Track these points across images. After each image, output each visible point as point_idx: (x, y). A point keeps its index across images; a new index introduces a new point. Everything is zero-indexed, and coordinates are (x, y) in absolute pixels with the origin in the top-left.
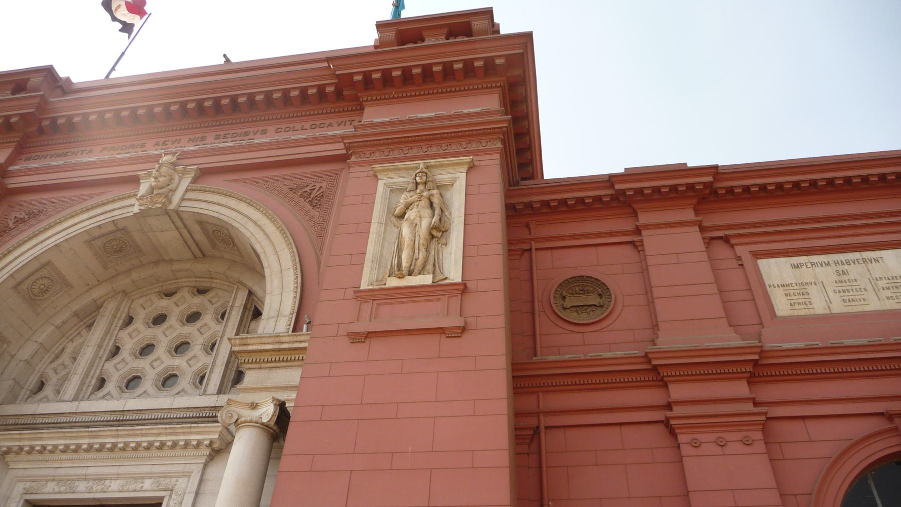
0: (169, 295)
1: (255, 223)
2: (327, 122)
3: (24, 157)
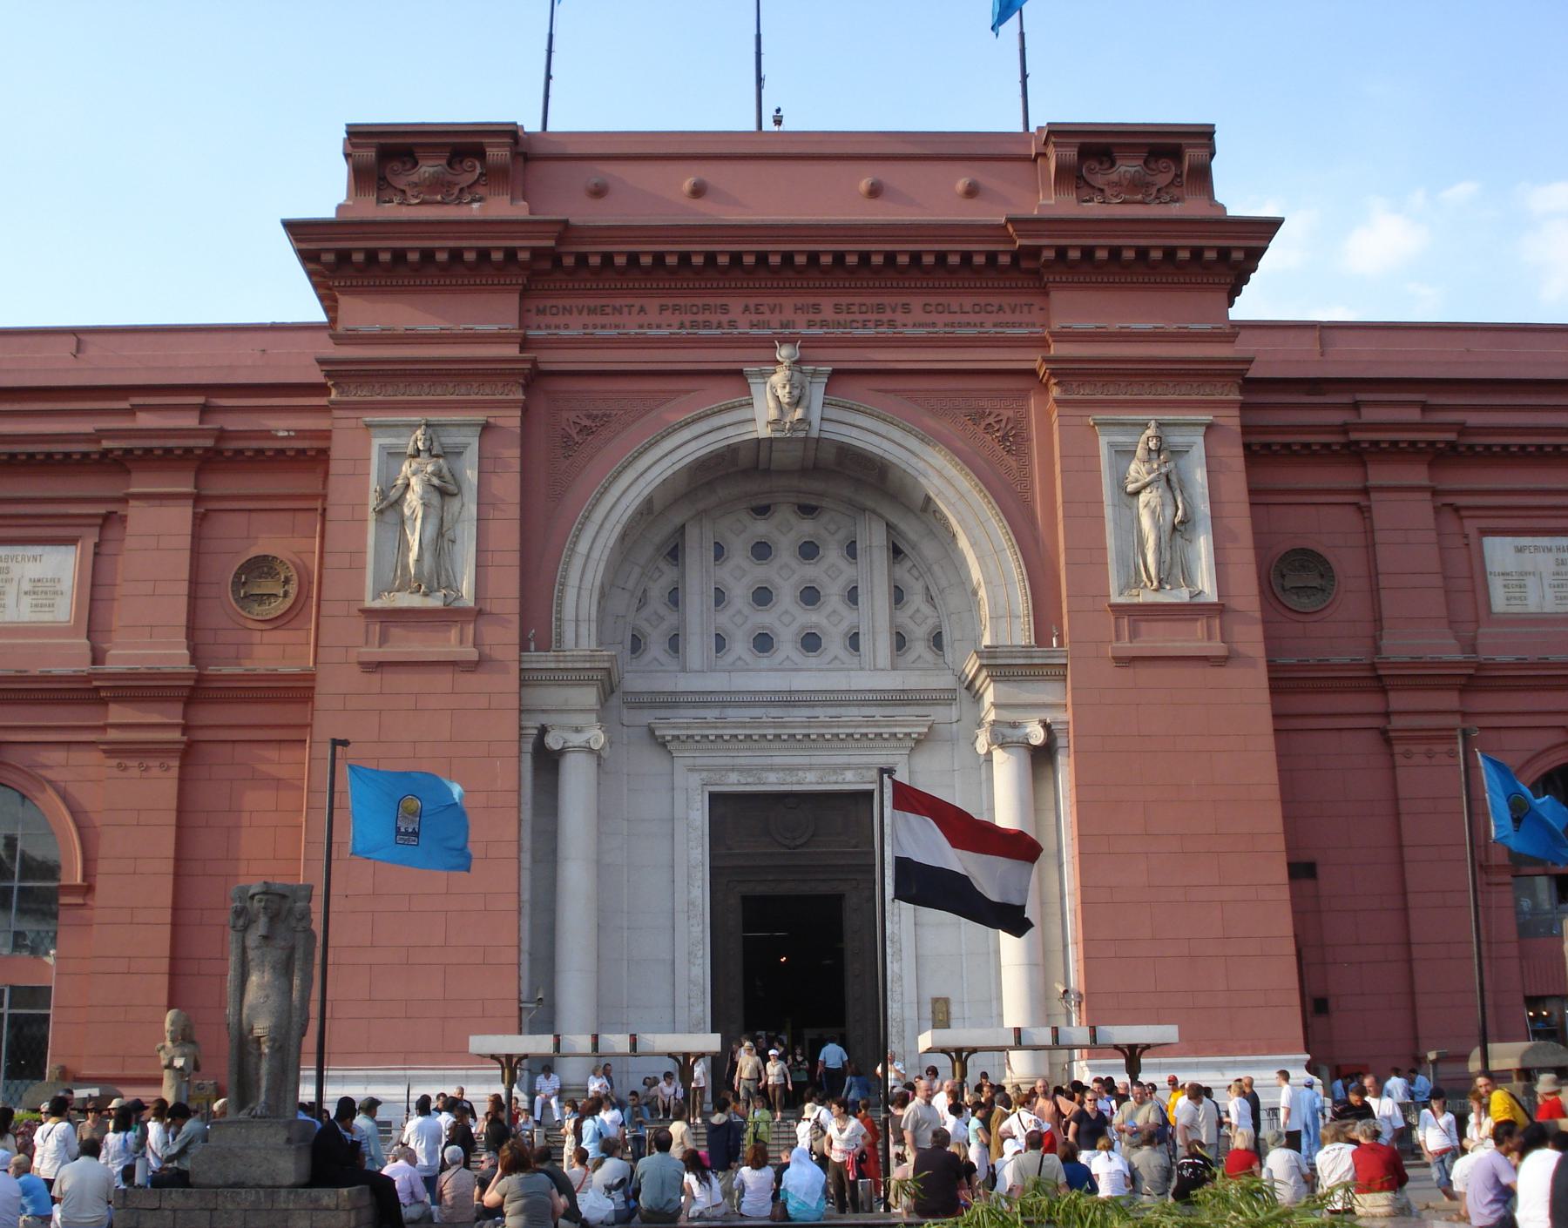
0: (762, 511)
1: (940, 473)
2: (995, 301)
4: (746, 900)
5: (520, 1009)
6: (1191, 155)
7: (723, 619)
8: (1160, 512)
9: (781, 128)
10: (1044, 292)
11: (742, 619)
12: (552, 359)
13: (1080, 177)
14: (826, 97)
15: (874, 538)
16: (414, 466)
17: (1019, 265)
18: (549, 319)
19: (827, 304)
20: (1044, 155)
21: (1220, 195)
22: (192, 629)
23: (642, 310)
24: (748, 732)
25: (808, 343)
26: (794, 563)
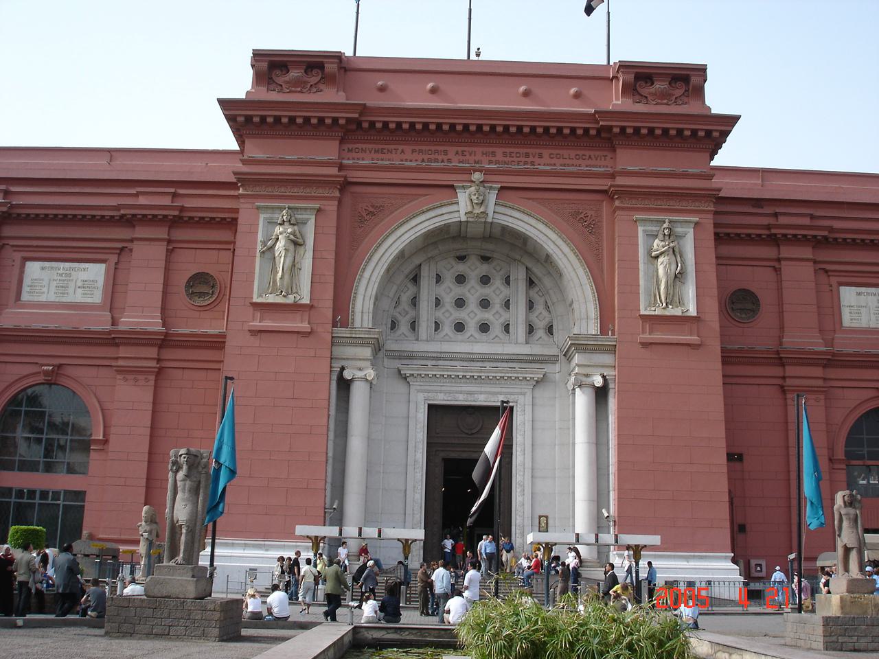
0: (462, 258)
1: (554, 242)
2: (587, 153)
3: (346, 147)
4: (446, 461)
5: (325, 512)
6: (694, 80)
7: (439, 314)
8: (669, 269)
9: (480, 58)
10: (613, 149)
11: (449, 314)
12: (355, 176)
13: (635, 90)
14: (502, 44)
15: (519, 275)
16: (281, 229)
17: (602, 134)
18: (354, 155)
19: (499, 152)
20: (617, 78)
21: (708, 103)
22: (164, 309)
23: (403, 151)
24: (449, 373)
25: (487, 172)
26: (478, 287)
